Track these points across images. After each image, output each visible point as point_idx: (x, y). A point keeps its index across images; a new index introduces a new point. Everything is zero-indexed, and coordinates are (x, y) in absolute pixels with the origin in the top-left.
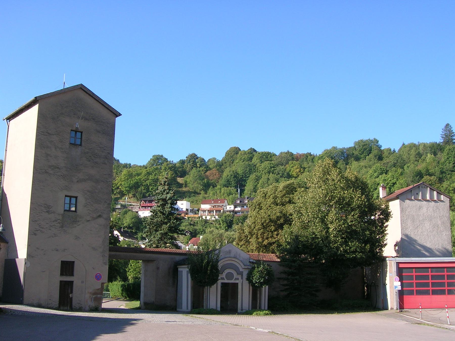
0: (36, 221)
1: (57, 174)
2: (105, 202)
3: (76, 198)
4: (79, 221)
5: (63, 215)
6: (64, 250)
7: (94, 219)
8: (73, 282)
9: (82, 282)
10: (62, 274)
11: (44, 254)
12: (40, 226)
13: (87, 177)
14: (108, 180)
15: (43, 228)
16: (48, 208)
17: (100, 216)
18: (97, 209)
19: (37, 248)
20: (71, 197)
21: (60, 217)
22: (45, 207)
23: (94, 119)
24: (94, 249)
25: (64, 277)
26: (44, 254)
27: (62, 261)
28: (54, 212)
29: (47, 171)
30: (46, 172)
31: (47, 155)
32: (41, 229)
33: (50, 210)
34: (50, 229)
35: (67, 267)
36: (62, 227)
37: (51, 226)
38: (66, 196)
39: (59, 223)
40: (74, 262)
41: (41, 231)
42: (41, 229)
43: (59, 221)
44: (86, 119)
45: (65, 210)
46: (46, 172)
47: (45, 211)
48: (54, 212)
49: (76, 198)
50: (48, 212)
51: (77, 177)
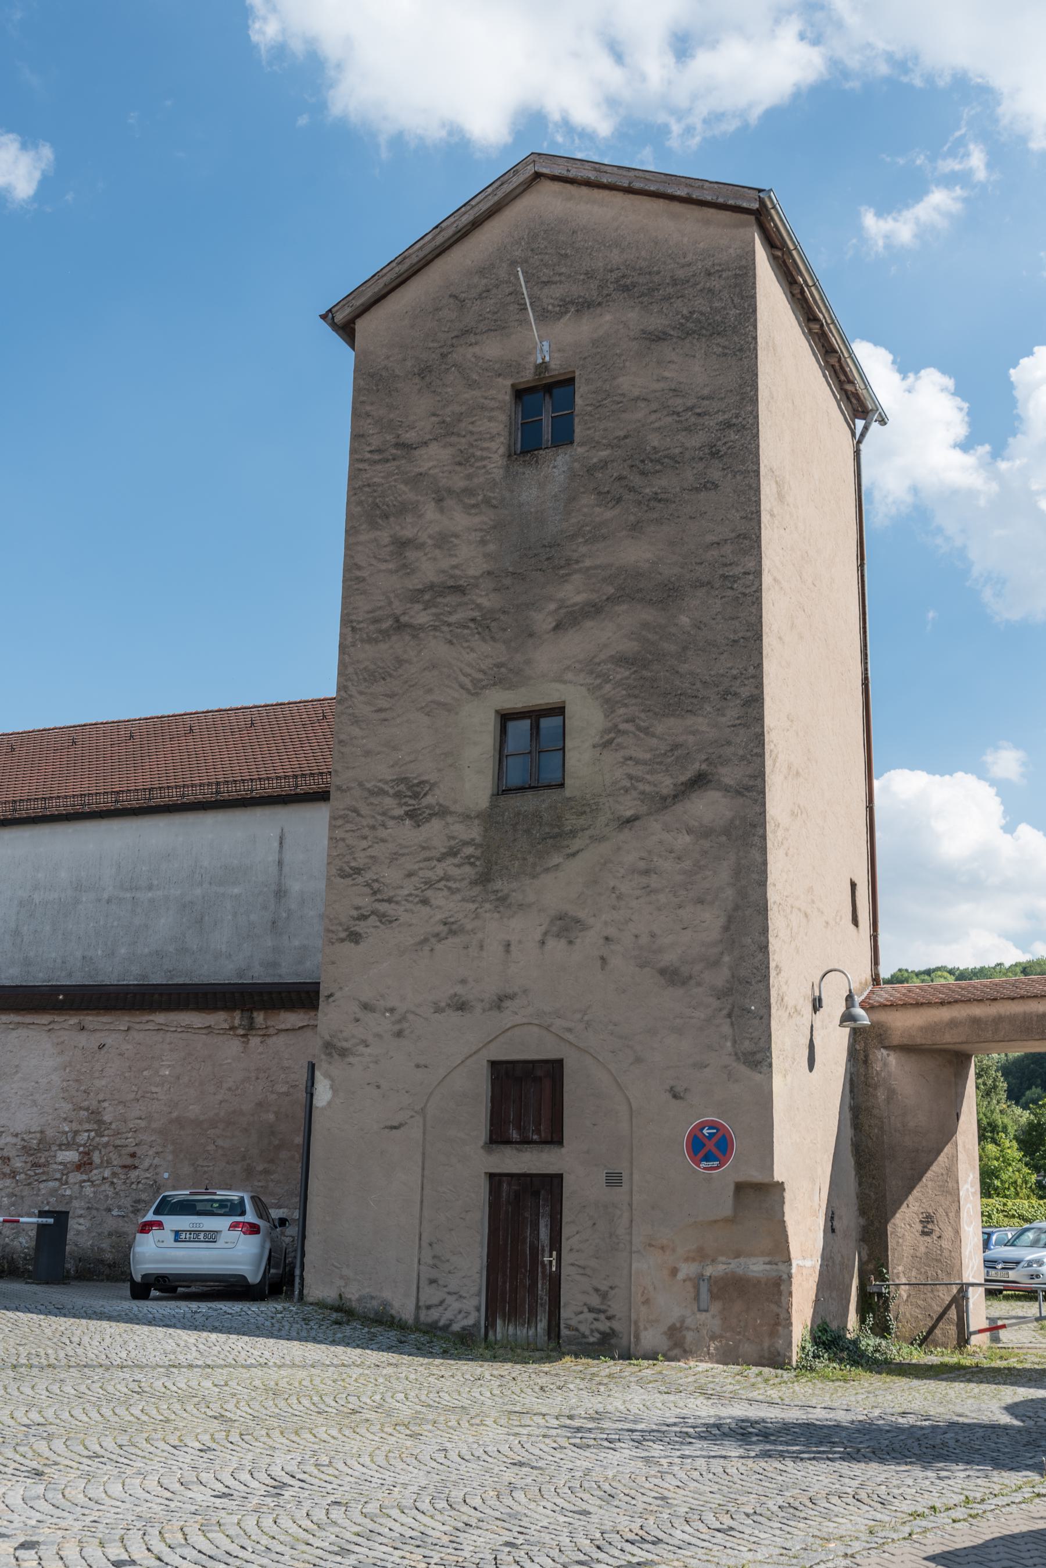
0: (358, 871)
1: (452, 619)
2: (726, 695)
3: (559, 711)
4: (573, 833)
5: (489, 818)
6: (500, 1002)
7: (665, 802)
8: (560, 1176)
9: (614, 1180)
10: (498, 1137)
11: (399, 1034)
12: (375, 893)
13: (611, 590)
14: (737, 570)
15: (389, 901)
16: (416, 796)
17: (699, 781)
18: (675, 747)
19: (366, 1007)
20: (535, 715)
21: (475, 832)
22: (398, 795)
23: (626, 289)
24: (672, 976)
25: (508, 1151)
26: (399, 1034)
27: (495, 1065)
28: (442, 812)
29: (404, 619)
30: (400, 626)
31: (402, 545)
32: (383, 907)
33: (425, 802)
34: (425, 902)
35: (526, 1096)
36: (484, 879)
37: (429, 884)
38: (505, 718)
39: (469, 861)
40: (559, 1064)
41: (382, 917)
42: (383, 907)
43: (469, 850)
44: (584, 306)
45: (502, 791)
46: (400, 626)
47: (400, 812)
48: (442, 812)
49: (559, 711)
50: (411, 815)
51: (552, 606)
